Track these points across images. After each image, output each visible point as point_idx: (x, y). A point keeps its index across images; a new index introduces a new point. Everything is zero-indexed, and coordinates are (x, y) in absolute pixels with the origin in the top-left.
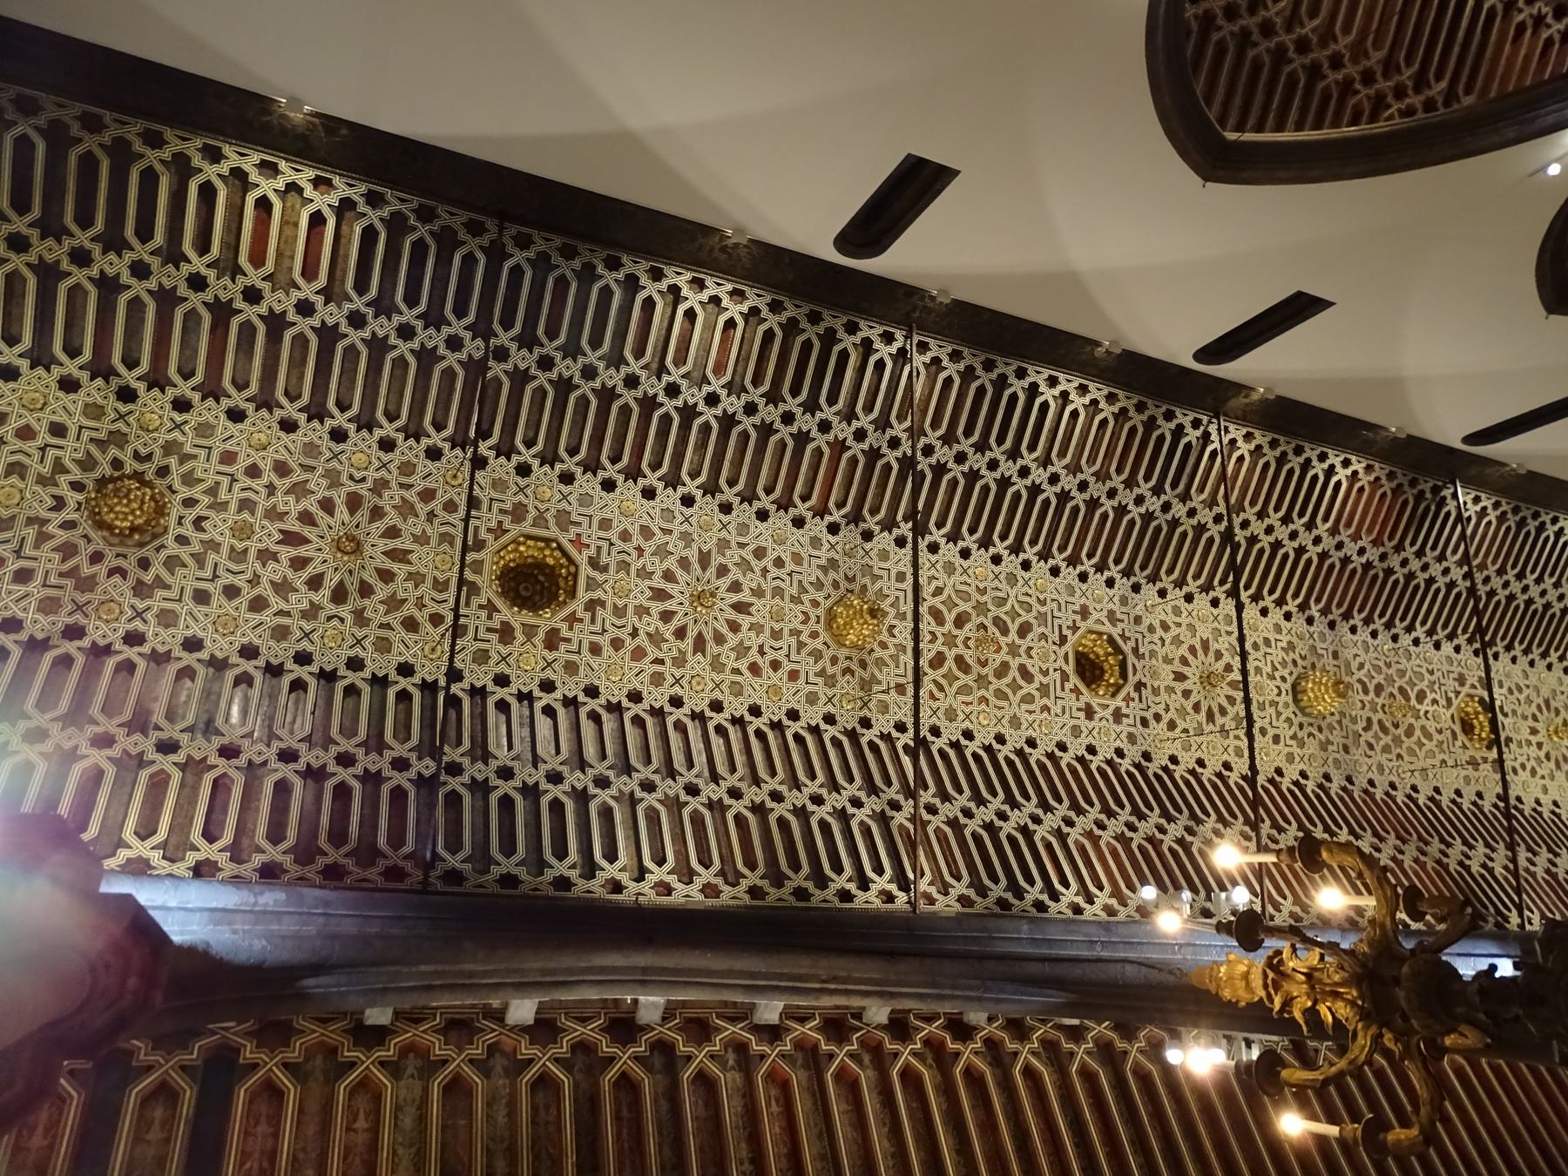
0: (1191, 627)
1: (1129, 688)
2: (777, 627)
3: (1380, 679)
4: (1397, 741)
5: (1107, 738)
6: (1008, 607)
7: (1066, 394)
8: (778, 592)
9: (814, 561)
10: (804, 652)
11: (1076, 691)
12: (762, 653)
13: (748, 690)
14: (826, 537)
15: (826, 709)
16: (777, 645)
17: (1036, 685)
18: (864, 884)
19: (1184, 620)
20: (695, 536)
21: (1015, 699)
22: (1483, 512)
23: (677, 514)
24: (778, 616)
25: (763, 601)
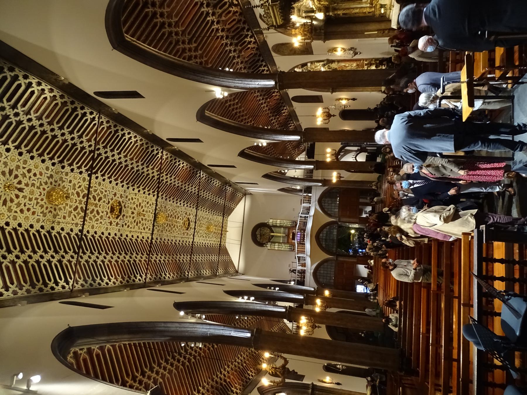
0: (138, 199)
1: (121, 217)
2: (31, 197)
3: (172, 213)
4: (172, 229)
5: (113, 230)
6: (97, 193)
7: (133, 138)
8: (33, 185)
9: (46, 175)
10: (38, 206)
11: (109, 217)
12: (25, 205)
13: (18, 218)
14: (51, 167)
15: (42, 224)
16: (30, 203)
17: (100, 216)
18: (57, 283)
19: (137, 197)
20: (9, 164)
21: (94, 220)
22: (203, 177)
23: (3, 155)
24: (32, 193)
25: (28, 188)
